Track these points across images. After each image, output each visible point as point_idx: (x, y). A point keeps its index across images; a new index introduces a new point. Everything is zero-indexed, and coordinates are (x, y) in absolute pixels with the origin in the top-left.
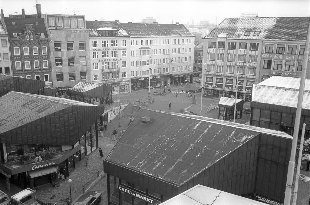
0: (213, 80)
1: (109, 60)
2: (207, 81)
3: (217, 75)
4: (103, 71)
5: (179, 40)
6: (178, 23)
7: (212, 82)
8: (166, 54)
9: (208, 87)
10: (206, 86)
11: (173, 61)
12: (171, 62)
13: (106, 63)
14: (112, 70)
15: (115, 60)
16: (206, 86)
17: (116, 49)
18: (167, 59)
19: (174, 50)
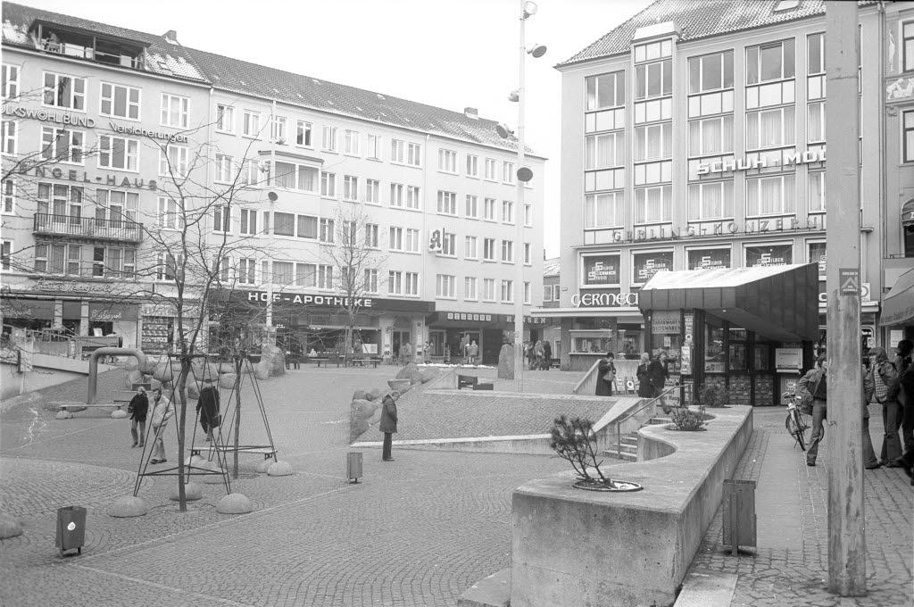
0: (618, 272)
1: (80, 177)
2: (587, 282)
3: (640, 240)
4: (36, 226)
5: (469, 158)
6: (475, 111)
7: (618, 282)
8: (404, 206)
9: (596, 306)
10: (582, 305)
11: (438, 240)
12: (432, 247)
13: (61, 189)
14: (99, 233)
15: (119, 181)
16: (582, 305)
17: (129, 133)
18: (409, 230)
19: (447, 197)
